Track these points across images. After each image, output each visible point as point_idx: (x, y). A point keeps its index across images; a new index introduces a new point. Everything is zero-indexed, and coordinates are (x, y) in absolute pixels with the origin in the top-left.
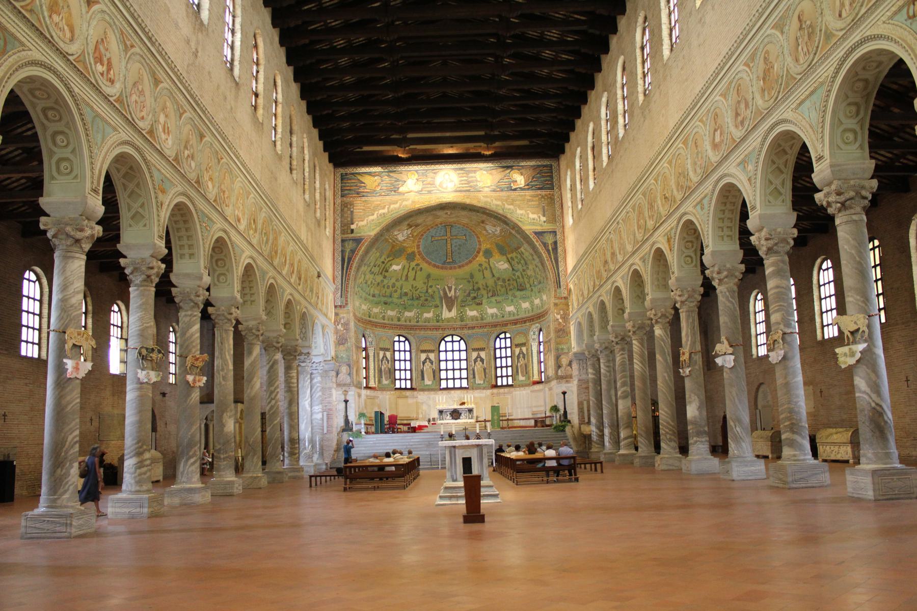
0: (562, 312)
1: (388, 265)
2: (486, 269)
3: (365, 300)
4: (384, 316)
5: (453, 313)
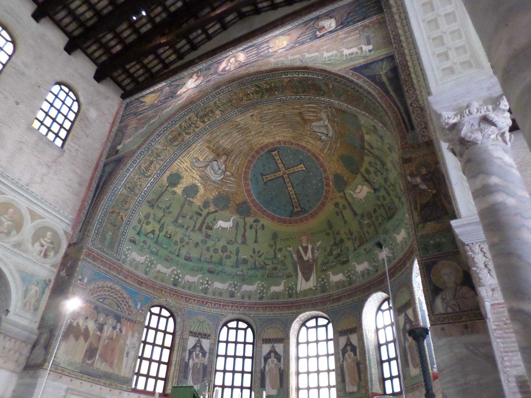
0: (424, 171)
1: (209, 219)
2: (344, 207)
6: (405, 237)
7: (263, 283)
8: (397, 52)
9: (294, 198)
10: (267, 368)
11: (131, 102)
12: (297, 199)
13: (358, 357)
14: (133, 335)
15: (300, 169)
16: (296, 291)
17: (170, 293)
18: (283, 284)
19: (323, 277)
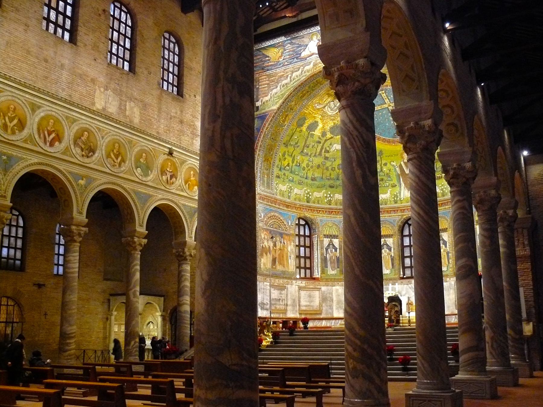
3: (299, 184)
4: (330, 201)
13: (448, 249)
14: (291, 244)
17: (306, 209)
18: (389, 192)
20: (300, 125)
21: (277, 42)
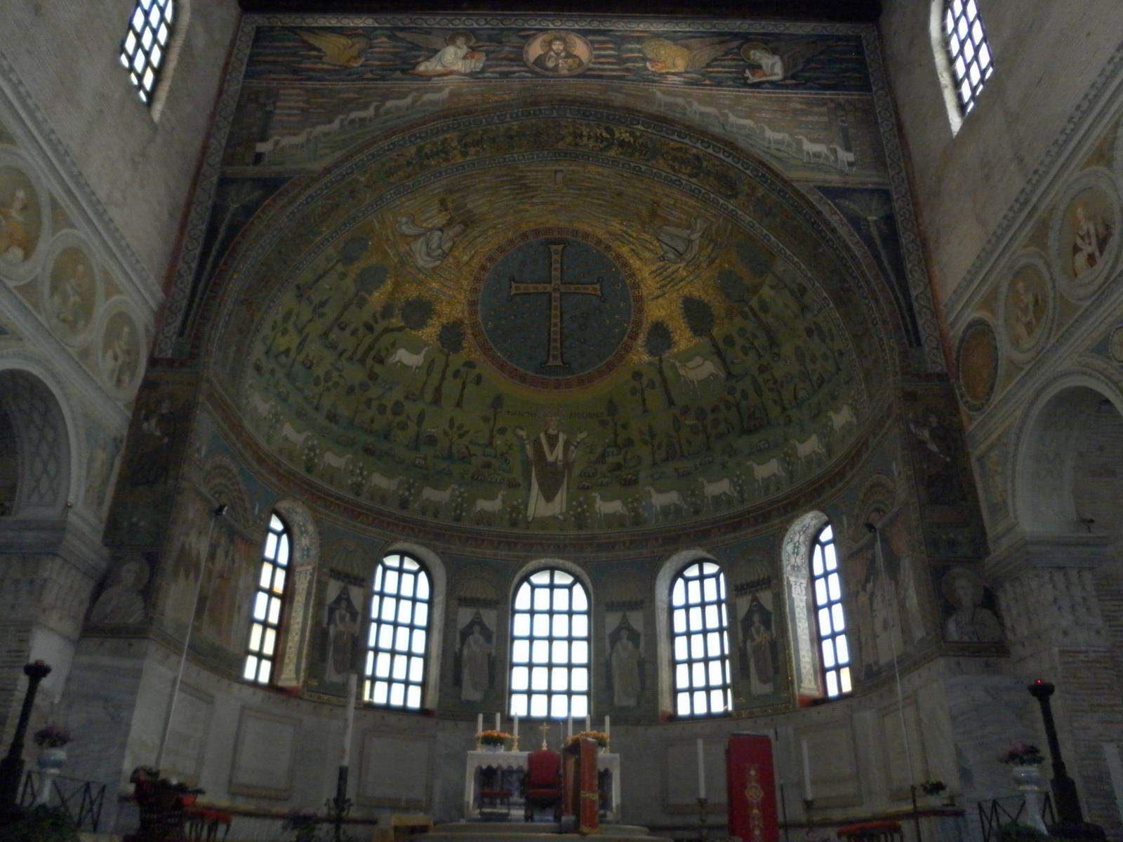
0: (933, 420)
2: (652, 384)
3: (300, 414)
4: (359, 485)
5: (558, 505)
6: (778, 473)
7: (462, 490)
8: (896, 188)
9: (555, 340)
10: (465, 652)
11: (272, 29)
12: (561, 344)
15: (589, 292)
16: (526, 517)
18: (500, 497)
19: (582, 499)
20: (348, 259)
21: (352, 25)
